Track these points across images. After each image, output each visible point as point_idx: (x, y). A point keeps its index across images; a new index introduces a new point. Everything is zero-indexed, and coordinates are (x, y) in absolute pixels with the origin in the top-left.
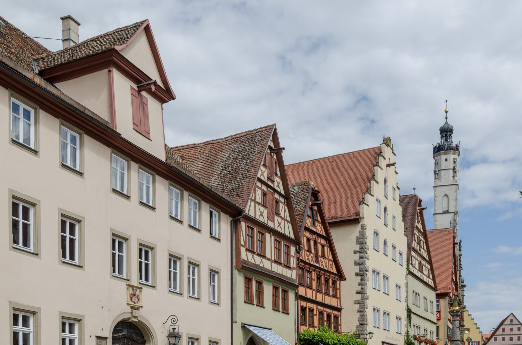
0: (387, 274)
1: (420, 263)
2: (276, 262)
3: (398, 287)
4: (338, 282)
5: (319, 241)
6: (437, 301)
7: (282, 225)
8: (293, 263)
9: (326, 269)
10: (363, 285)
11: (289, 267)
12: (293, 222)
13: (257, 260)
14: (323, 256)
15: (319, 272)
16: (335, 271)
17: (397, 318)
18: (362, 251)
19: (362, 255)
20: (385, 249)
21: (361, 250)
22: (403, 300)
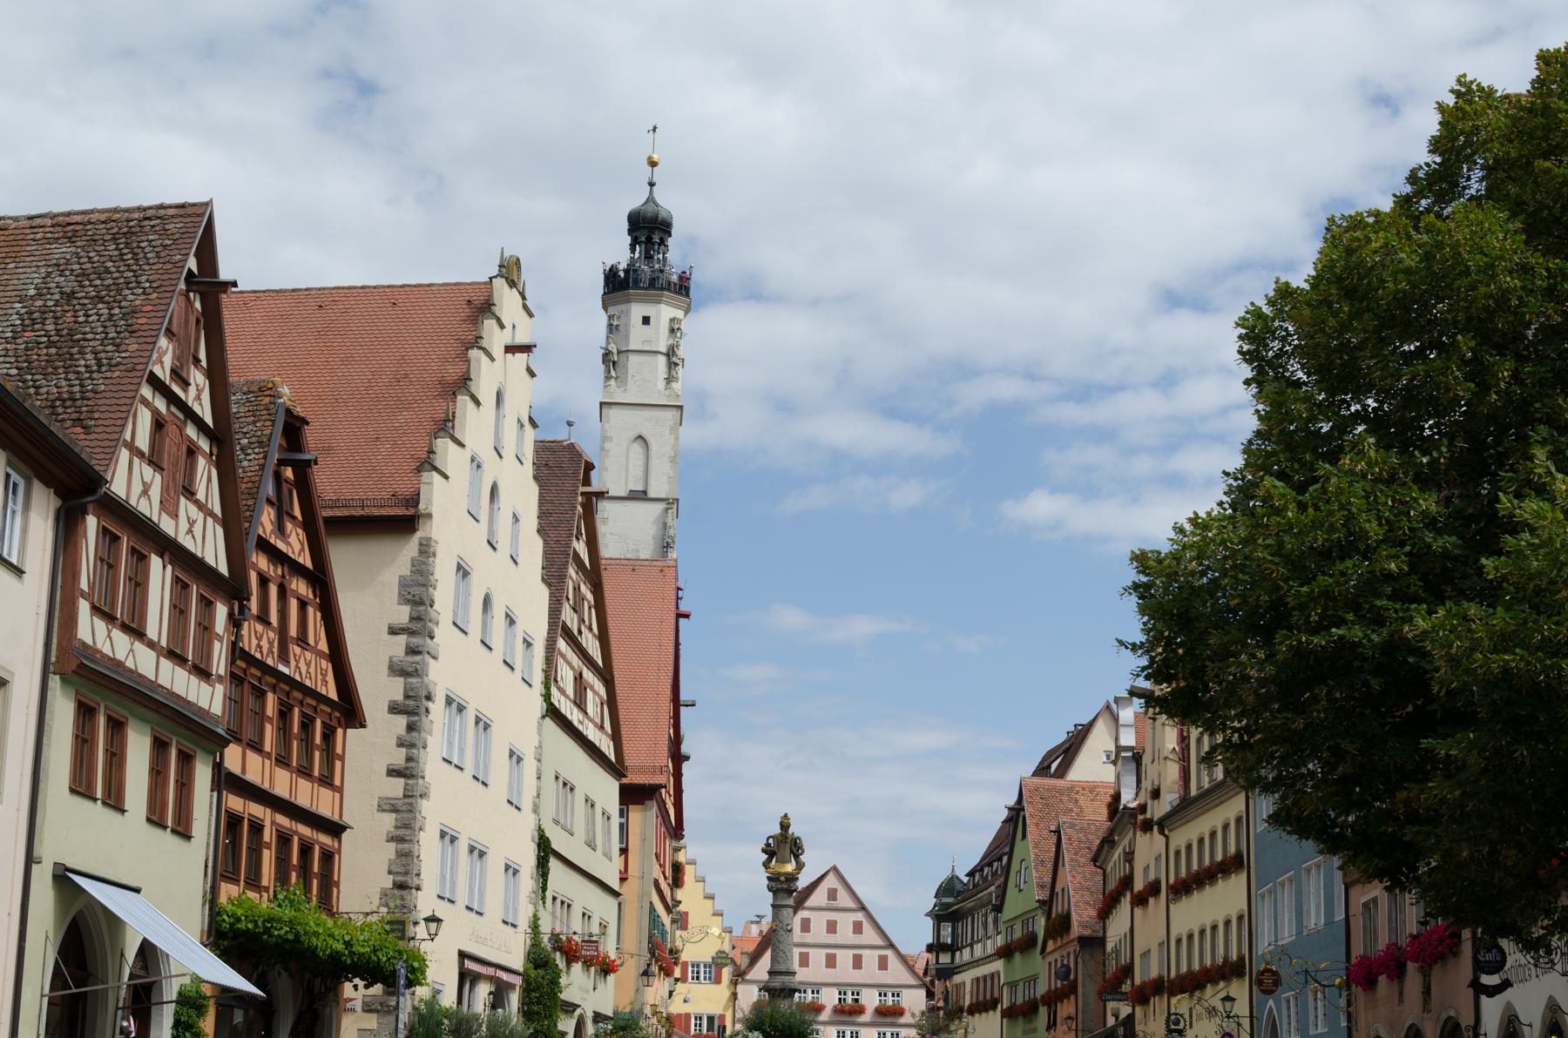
1: (579, 678)
3: (515, 757)
4: (340, 731)
5: (294, 586)
6: (621, 815)
9: (308, 683)
10: (412, 745)
11: (203, 673)
14: (302, 640)
15: (288, 694)
16: (333, 695)
17: (507, 867)
19: (415, 641)
21: (415, 626)
22: (527, 805)
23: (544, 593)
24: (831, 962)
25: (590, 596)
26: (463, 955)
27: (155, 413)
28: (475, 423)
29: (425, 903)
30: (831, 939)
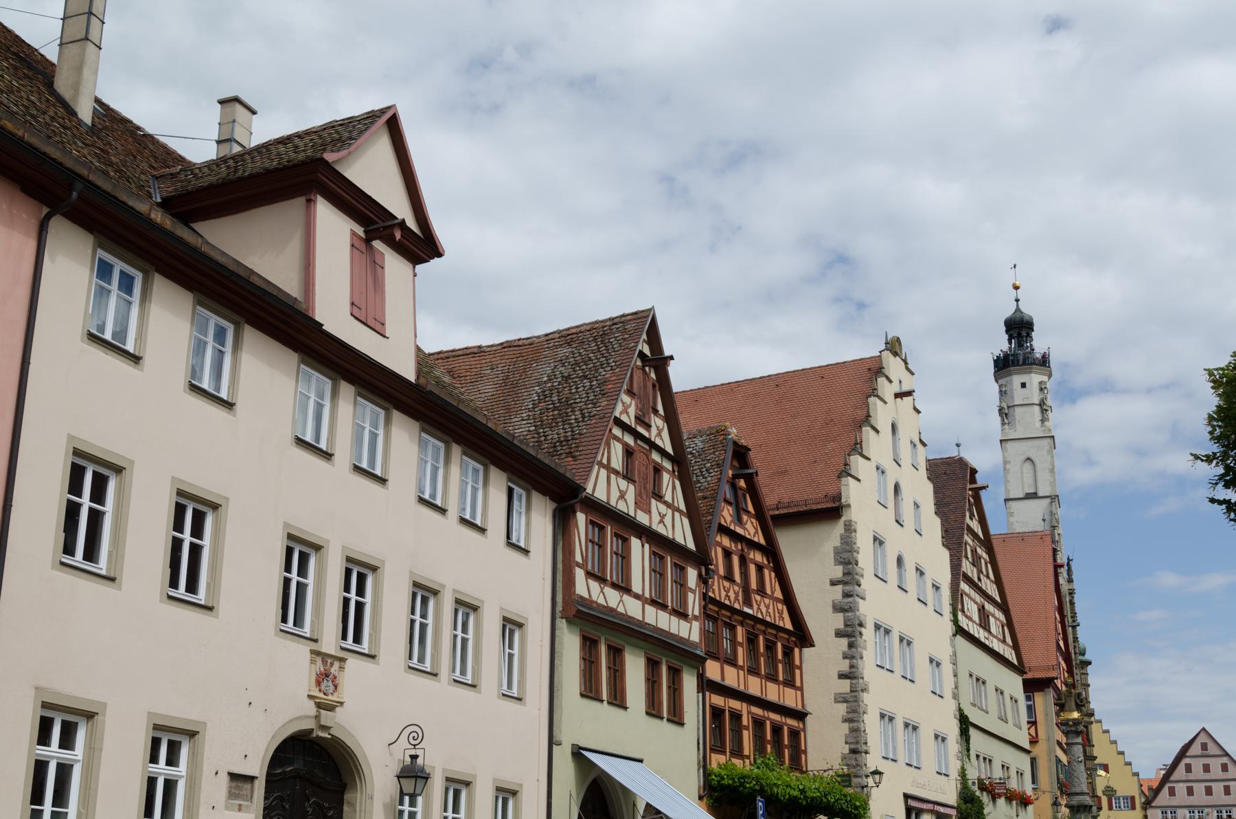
0: (909, 633)
1: (982, 610)
2: (653, 602)
4: (797, 650)
5: (751, 556)
6: (1028, 698)
7: (668, 520)
8: (694, 604)
9: (768, 619)
10: (853, 657)
11: (682, 615)
12: (692, 513)
13: (612, 598)
14: (761, 591)
15: (753, 627)
16: (789, 626)
17: (936, 737)
18: (849, 579)
19: (848, 588)
20: (900, 577)
21: (847, 579)
22: (948, 694)
23: (945, 555)
24: (1209, 791)
25: (985, 555)
26: (907, 797)
27: (625, 445)
28: (877, 444)
29: (873, 761)
30: (1207, 776)
